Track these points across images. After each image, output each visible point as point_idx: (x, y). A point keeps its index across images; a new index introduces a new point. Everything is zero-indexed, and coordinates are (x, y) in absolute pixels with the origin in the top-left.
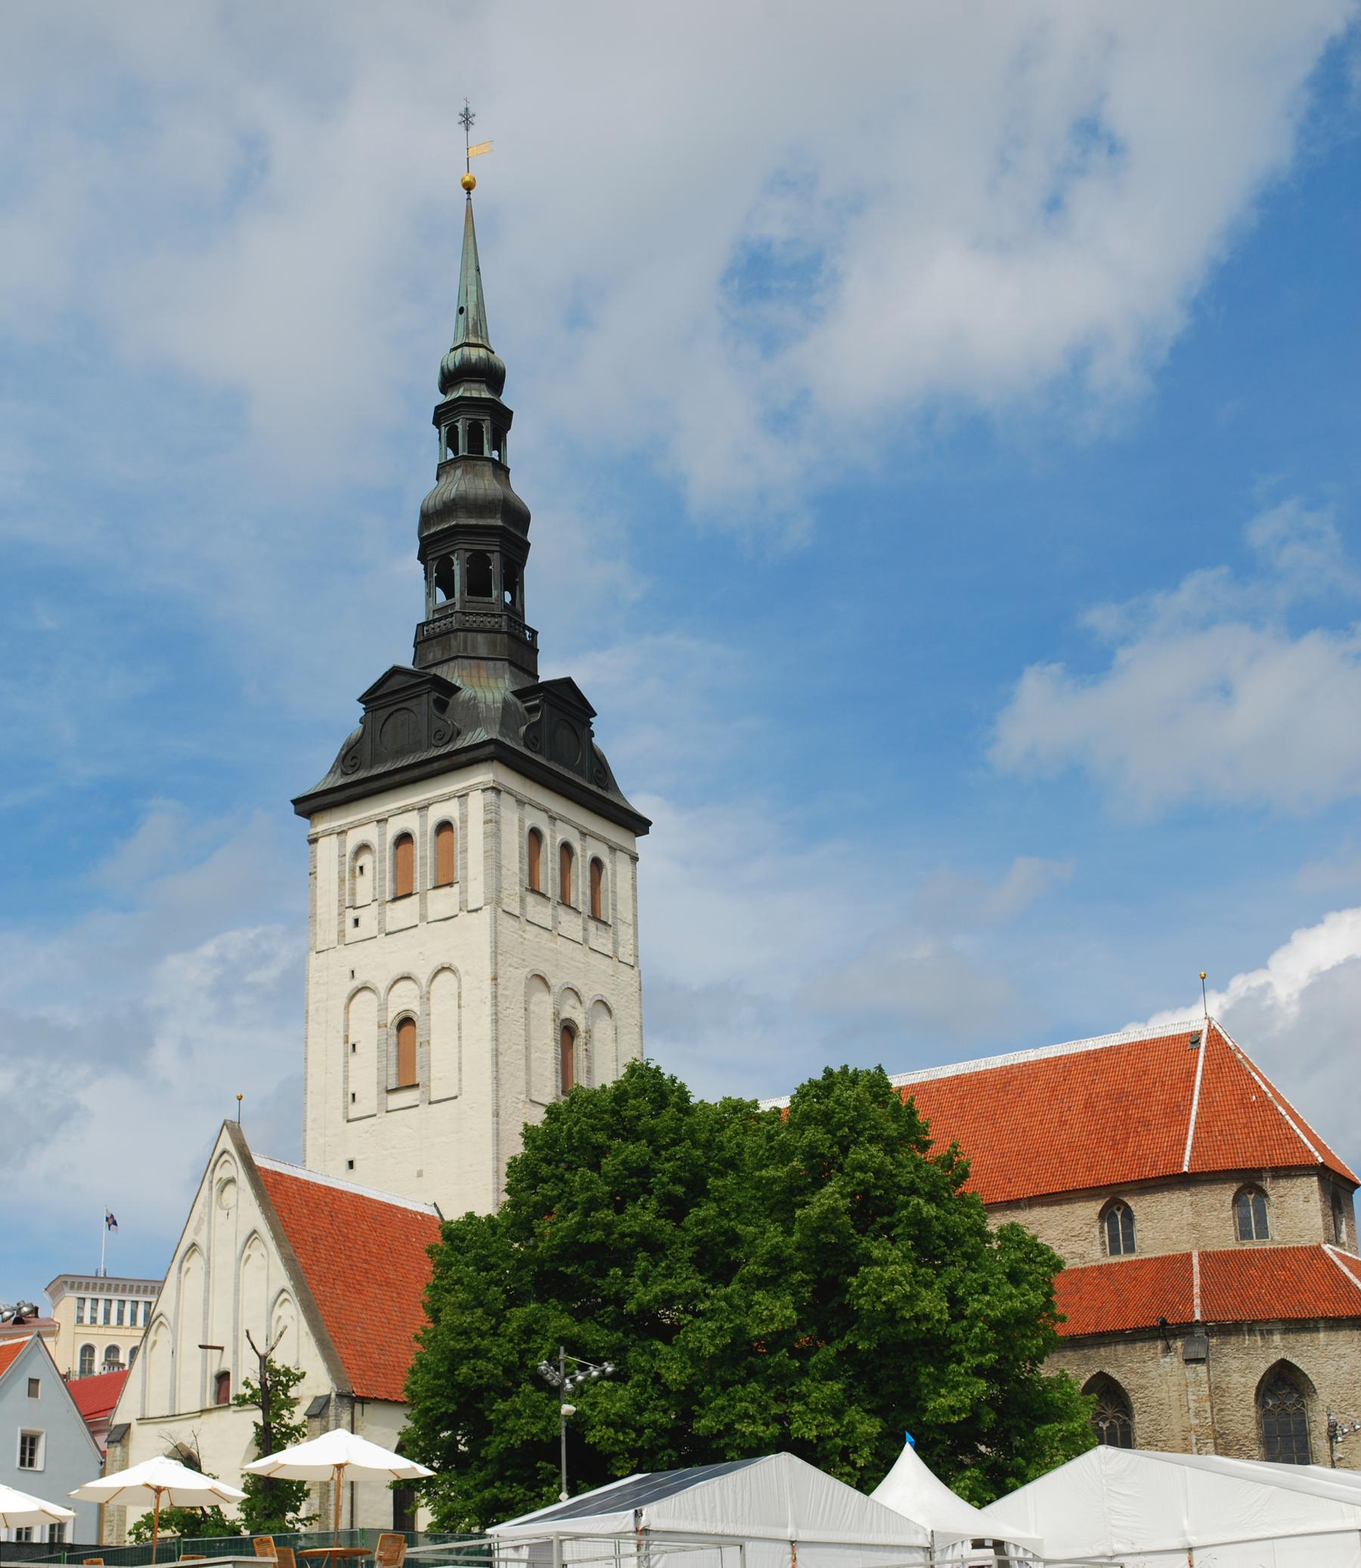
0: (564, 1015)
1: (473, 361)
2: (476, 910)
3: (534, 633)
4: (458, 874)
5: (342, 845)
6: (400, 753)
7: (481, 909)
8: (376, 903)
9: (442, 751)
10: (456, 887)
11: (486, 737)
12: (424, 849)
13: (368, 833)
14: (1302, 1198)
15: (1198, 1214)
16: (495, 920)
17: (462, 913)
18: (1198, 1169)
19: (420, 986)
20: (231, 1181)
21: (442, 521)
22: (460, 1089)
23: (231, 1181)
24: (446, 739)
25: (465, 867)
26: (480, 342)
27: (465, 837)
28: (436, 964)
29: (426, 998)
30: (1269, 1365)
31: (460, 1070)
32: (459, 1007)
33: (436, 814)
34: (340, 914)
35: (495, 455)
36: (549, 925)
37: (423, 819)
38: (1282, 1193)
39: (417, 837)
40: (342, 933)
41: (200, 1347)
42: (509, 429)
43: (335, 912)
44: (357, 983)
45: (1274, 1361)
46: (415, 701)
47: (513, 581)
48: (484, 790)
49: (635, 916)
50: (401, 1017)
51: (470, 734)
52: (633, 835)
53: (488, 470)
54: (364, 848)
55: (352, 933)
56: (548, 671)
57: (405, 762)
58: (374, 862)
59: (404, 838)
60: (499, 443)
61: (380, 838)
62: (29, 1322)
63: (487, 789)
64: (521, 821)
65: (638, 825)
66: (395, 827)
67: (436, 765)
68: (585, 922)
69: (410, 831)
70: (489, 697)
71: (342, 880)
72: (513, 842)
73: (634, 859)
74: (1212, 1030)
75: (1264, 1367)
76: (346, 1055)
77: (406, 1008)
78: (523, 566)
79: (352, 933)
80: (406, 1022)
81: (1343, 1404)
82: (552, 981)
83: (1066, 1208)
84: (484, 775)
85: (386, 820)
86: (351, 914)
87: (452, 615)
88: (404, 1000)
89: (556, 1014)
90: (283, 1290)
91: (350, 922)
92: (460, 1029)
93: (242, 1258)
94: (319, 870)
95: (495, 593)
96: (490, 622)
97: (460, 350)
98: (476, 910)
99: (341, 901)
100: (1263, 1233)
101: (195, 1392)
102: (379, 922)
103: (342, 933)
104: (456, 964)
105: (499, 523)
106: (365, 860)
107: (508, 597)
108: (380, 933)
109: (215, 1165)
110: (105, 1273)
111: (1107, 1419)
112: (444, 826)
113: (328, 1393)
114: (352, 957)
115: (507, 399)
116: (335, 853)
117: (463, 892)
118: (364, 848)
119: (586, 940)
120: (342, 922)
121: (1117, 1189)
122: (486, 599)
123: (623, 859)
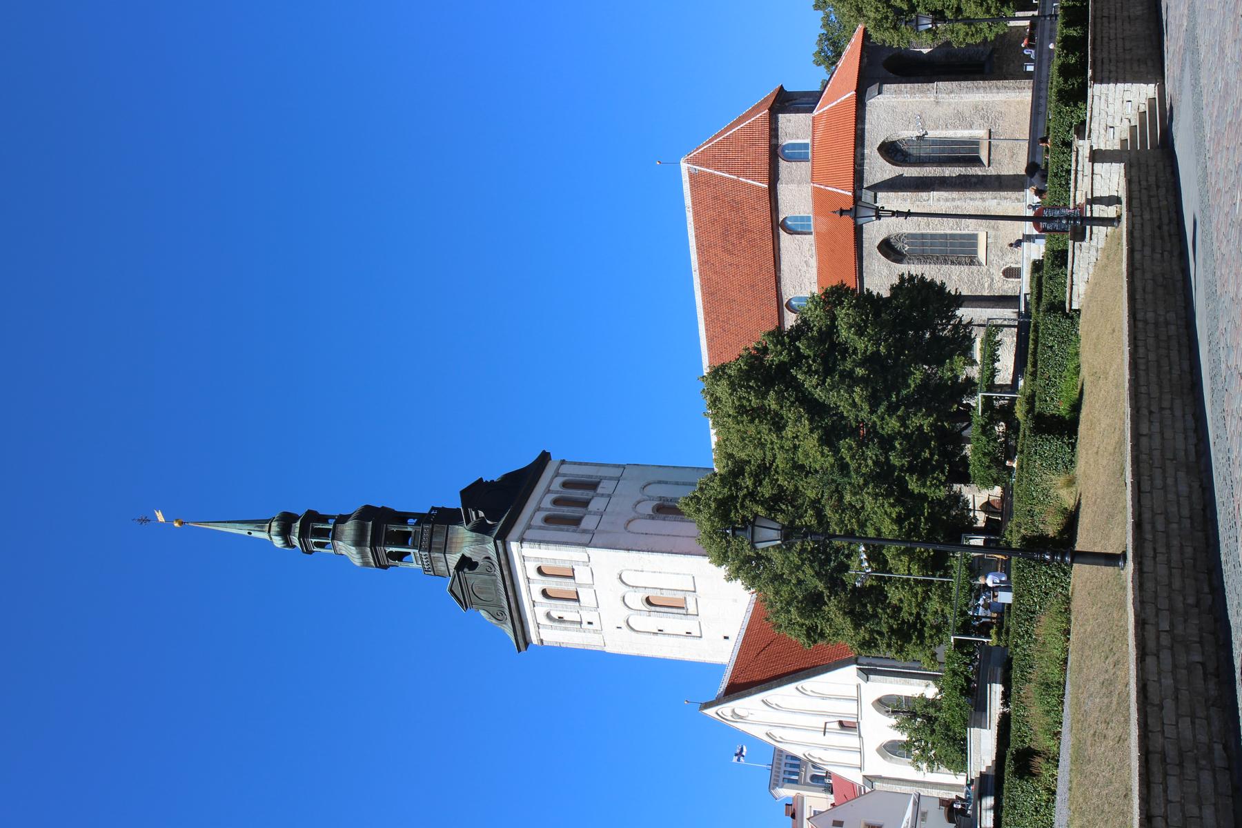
0: (652, 513)
1: (279, 530)
2: (589, 557)
3: (433, 508)
4: (568, 565)
6: (497, 590)
7: (588, 555)
9: (498, 568)
11: (492, 543)
12: (552, 584)
13: (541, 611)
14: (788, 124)
15: (792, 181)
16: (595, 547)
17: (590, 566)
18: (767, 180)
19: (628, 591)
20: (733, 711)
22: (689, 575)
23: (733, 711)
24: (492, 566)
26: (268, 524)
28: (618, 582)
30: (880, 157)
31: (678, 574)
32: (642, 571)
33: (533, 574)
34: (584, 632)
35: (332, 521)
36: (598, 518)
38: (785, 134)
39: (544, 586)
40: (595, 631)
41: (824, 735)
42: (316, 512)
43: (584, 634)
44: (624, 625)
45: (878, 154)
47: (402, 518)
48: (522, 548)
49: (597, 465)
50: (645, 603)
51: (489, 552)
52: (550, 461)
53: (340, 527)
54: (548, 616)
55: (596, 626)
56: (455, 503)
57: (503, 589)
60: (324, 519)
61: (544, 606)
62: (794, 809)
63: (521, 546)
64: (540, 528)
65: (544, 458)
66: (538, 597)
67: (506, 573)
68: (598, 495)
70: (468, 539)
71: (566, 629)
72: (550, 534)
73: (563, 462)
74: (688, 161)
75: (881, 160)
77: (640, 598)
78: (394, 510)
80: (648, 601)
81: (904, 119)
82: (630, 517)
83: (783, 251)
84: (514, 546)
85: (534, 602)
86: (585, 625)
87: (420, 555)
88: (636, 600)
89: (651, 517)
90: (797, 688)
91: (590, 626)
92: (655, 572)
93: (778, 708)
95: (409, 529)
96: (426, 534)
97: (272, 537)
98: (589, 557)
100: (805, 146)
101: (850, 740)
103: (595, 631)
104: (618, 571)
105: (371, 523)
106: (555, 615)
107: (410, 521)
109: (724, 718)
110: (770, 765)
111: (903, 246)
112: (540, 571)
113: (856, 669)
115: (301, 512)
116: (550, 631)
117: (577, 562)
118: (548, 616)
119: (610, 496)
121: (775, 224)
122: (413, 535)
123: (565, 469)
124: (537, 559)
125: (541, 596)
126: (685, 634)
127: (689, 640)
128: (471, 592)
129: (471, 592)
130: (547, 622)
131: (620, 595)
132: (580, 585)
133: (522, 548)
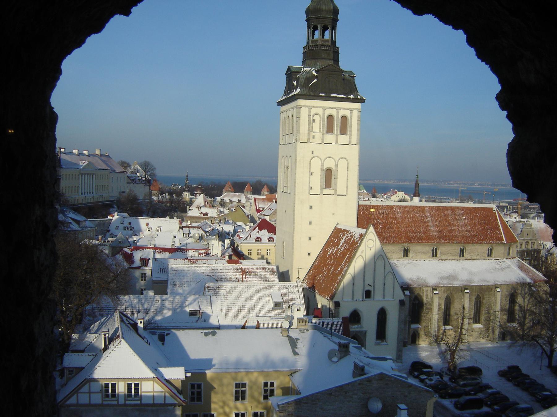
5: (310, 112)
8: (321, 133)
10: (348, 136)
13: (320, 111)
25: (351, 131)
27: (351, 123)
29: (336, 165)
32: (348, 171)
34: (308, 133)
37: (338, 112)
55: (312, 140)
59: (330, 117)
66: (328, 112)
76: (310, 176)
79: (312, 140)
91: (311, 137)
94: (301, 117)
99: (309, 129)
102: (322, 139)
108: (323, 142)
112: (344, 118)
114: (313, 147)
124: (351, 117)
126: (311, 186)
127: (307, 188)
131: (333, 157)
132: (337, 135)
133: (358, 111)
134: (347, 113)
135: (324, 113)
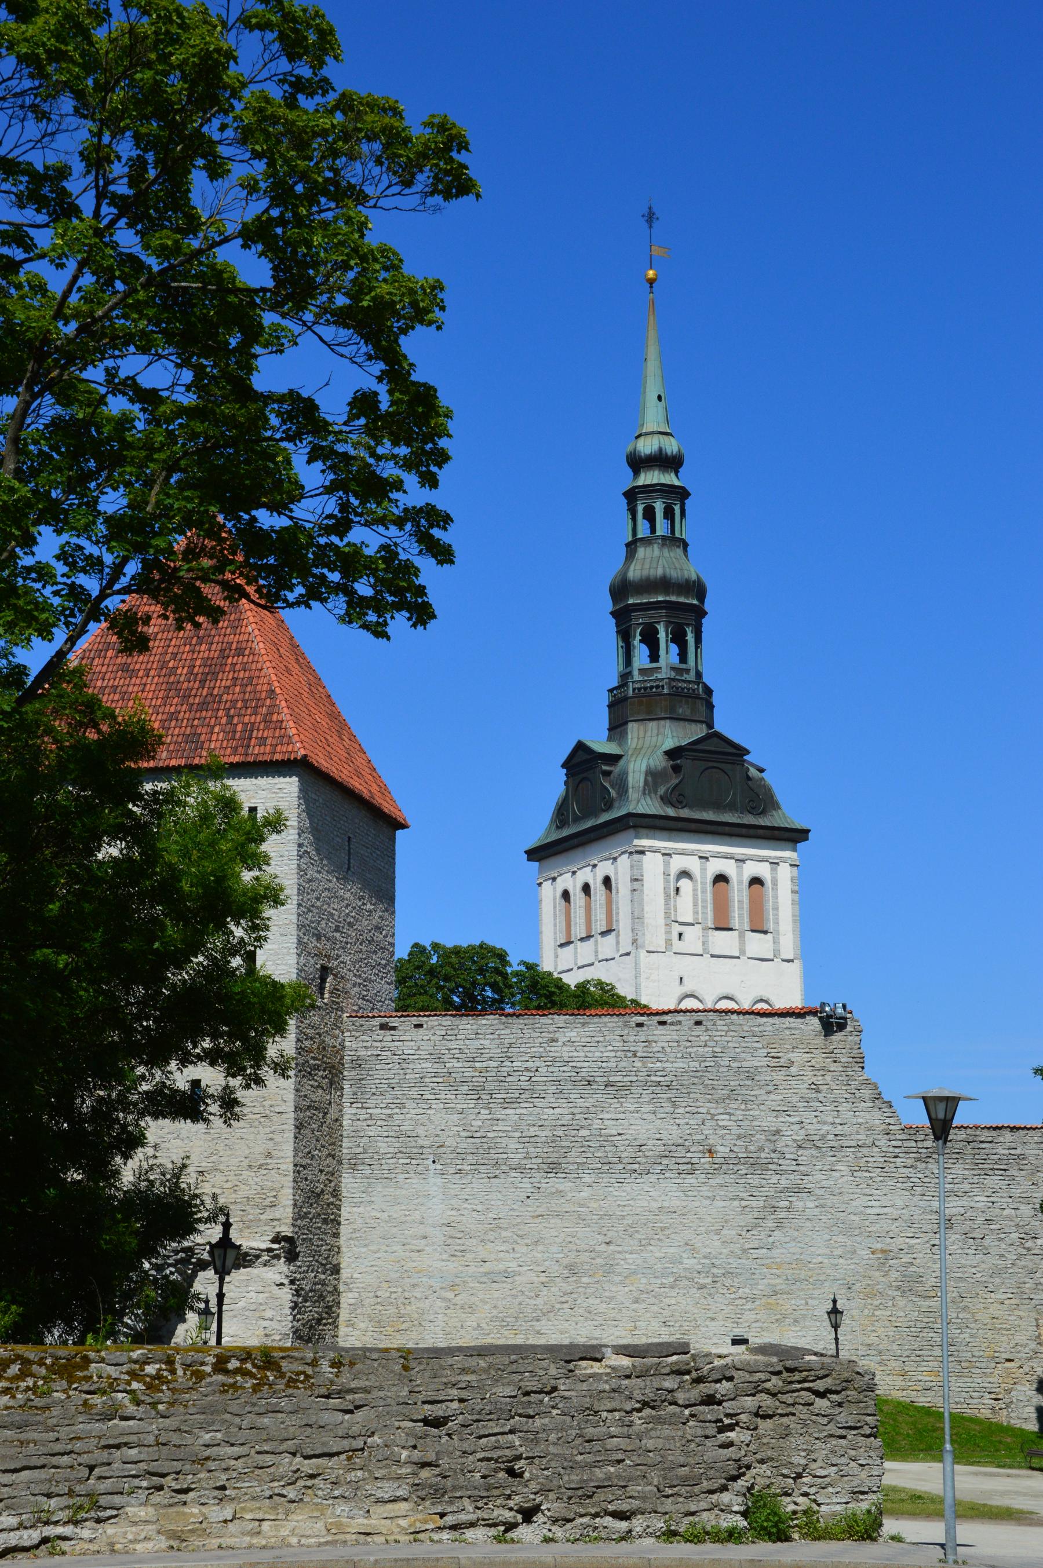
2: (788, 961)
10: (769, 936)
13: (693, 864)
21: (679, 594)
33: (752, 869)
34: (667, 925)
37: (740, 870)
40: (669, 942)
46: (729, 766)
54: (685, 874)
55: (678, 946)
58: (695, 890)
69: (727, 875)
79: (678, 946)
91: (676, 936)
94: (645, 878)
98: (788, 961)
99: (667, 915)
102: (703, 944)
106: (685, 884)
108: (706, 950)
112: (756, 881)
118: (685, 874)
120: (668, 932)
125: (718, 873)
128: (711, 764)
129: (711, 764)
130: (674, 871)
133: (791, 865)
134: (762, 870)
135: (704, 870)
